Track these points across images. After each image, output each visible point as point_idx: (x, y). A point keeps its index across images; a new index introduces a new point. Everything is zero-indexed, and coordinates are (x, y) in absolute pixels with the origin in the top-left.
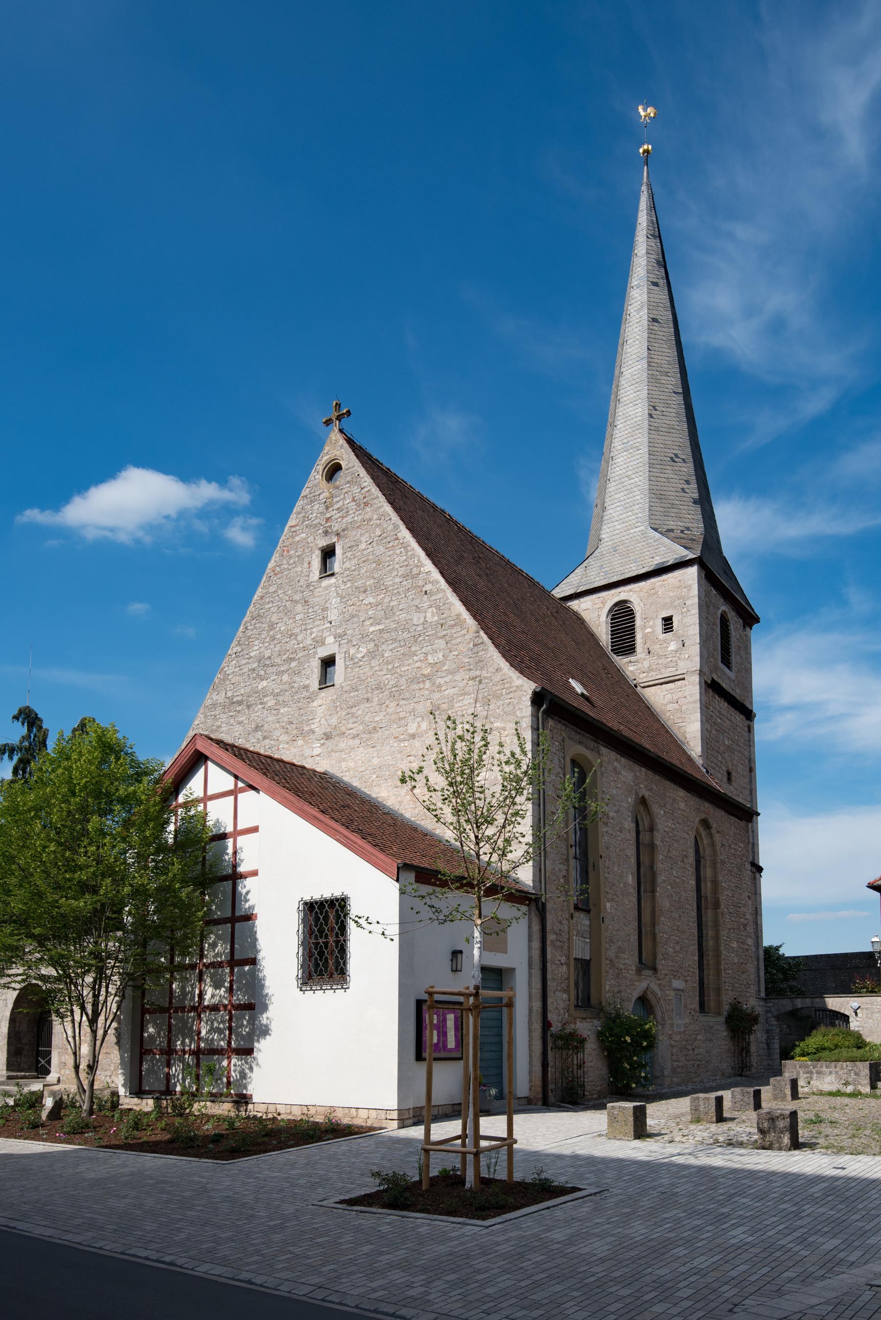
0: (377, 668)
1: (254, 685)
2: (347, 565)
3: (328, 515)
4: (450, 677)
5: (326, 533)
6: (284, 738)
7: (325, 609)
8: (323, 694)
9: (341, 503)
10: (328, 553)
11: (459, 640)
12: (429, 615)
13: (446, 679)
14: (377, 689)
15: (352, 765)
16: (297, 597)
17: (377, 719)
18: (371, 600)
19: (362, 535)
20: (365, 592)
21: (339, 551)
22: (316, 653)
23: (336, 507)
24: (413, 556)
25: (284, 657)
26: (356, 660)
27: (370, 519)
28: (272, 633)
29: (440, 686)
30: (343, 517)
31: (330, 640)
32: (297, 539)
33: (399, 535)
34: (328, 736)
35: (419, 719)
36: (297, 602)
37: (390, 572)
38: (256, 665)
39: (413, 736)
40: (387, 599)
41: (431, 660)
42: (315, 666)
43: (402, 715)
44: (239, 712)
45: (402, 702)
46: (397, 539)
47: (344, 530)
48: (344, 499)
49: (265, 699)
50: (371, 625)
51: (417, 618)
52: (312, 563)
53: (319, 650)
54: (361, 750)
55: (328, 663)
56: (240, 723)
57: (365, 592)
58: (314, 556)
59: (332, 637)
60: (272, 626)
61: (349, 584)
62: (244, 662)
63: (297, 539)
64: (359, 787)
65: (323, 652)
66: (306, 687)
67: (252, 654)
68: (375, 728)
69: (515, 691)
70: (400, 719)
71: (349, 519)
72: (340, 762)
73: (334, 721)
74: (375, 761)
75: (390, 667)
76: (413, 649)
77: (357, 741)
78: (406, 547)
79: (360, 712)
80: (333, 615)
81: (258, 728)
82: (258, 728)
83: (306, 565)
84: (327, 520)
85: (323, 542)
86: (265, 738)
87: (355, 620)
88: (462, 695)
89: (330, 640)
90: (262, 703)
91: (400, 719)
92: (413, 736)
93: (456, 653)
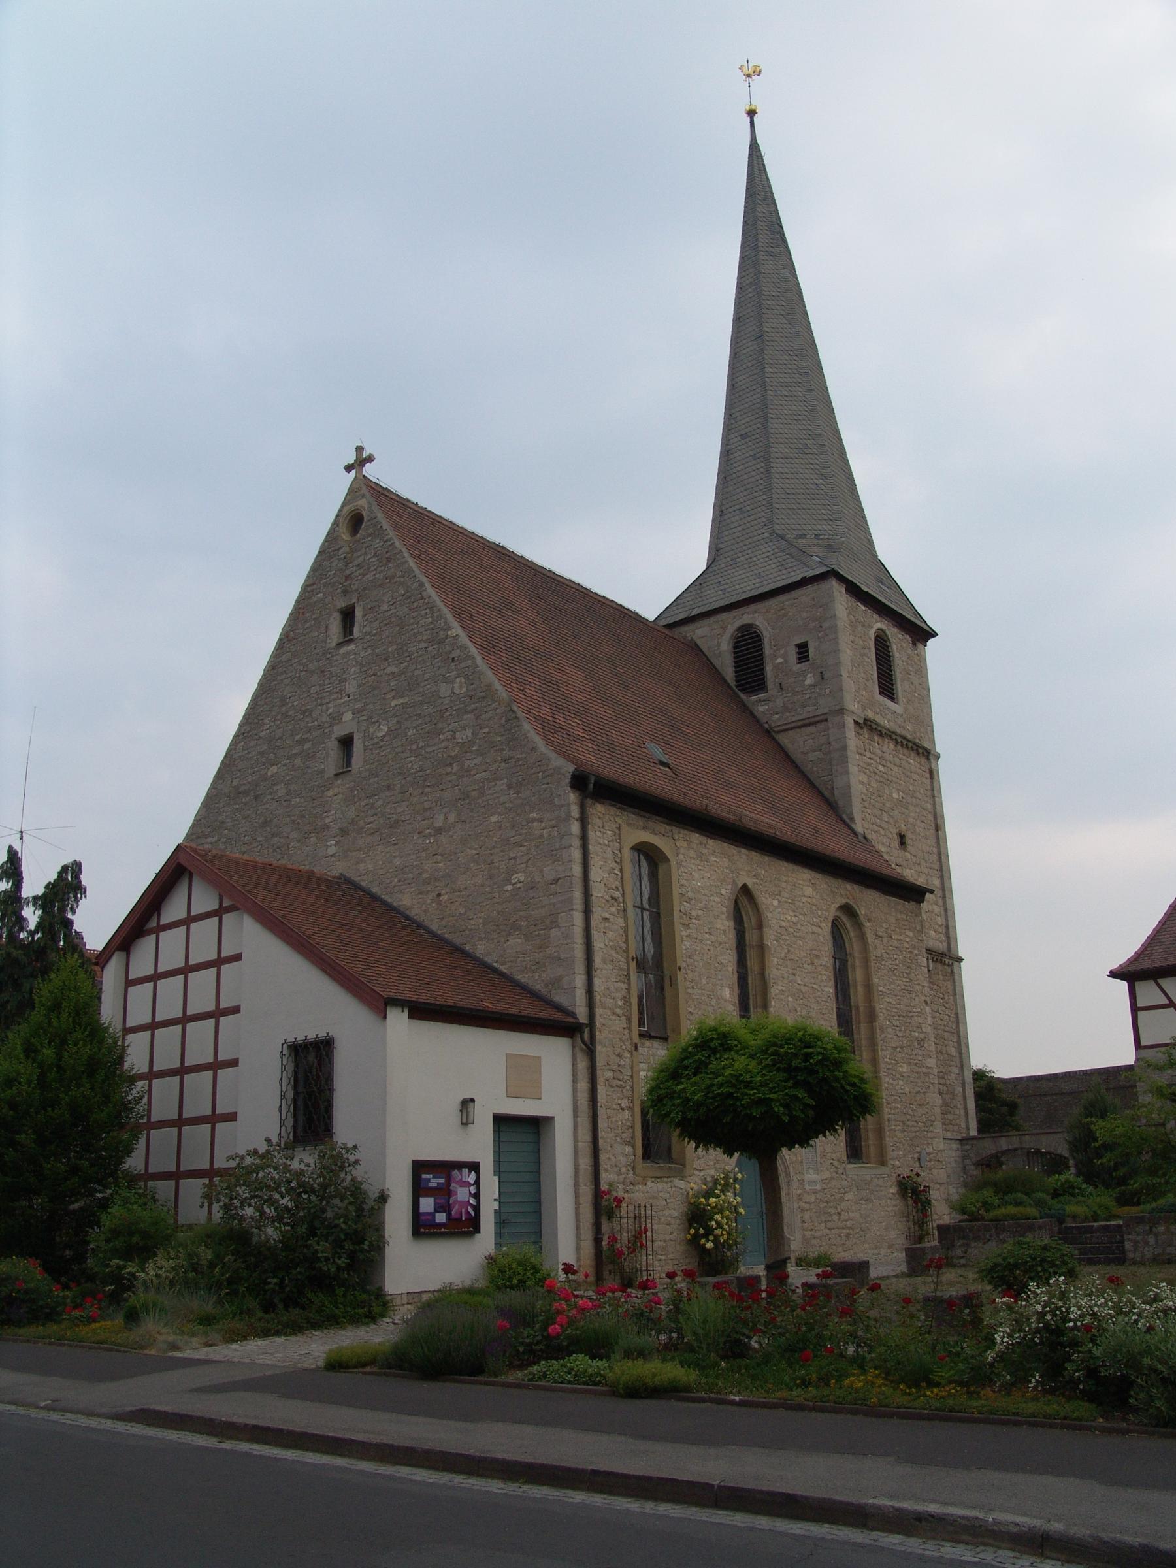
0: (400, 749)
1: (263, 772)
2: (367, 629)
3: (348, 572)
4: (480, 758)
5: (345, 592)
6: (295, 835)
7: (345, 680)
8: (339, 782)
9: (361, 558)
10: (348, 616)
11: (490, 714)
12: (456, 685)
13: (475, 761)
14: (399, 774)
15: (371, 867)
16: (311, 667)
17: (399, 810)
18: (393, 669)
19: (384, 594)
20: (386, 659)
21: (358, 613)
22: (332, 732)
23: (356, 563)
24: (441, 617)
25: (297, 737)
26: (376, 740)
27: (393, 577)
28: (284, 709)
29: (469, 770)
30: (364, 575)
31: (348, 716)
32: (314, 599)
33: (424, 594)
34: (344, 832)
35: (445, 810)
36: (312, 672)
37: (415, 635)
38: (265, 747)
39: (439, 831)
40: (412, 668)
41: (459, 737)
42: (332, 746)
43: (427, 805)
44: (245, 804)
45: (428, 789)
46: (423, 598)
47: (365, 589)
48: (365, 554)
49: (275, 788)
50: (394, 698)
51: (444, 690)
52: (330, 626)
53: (335, 728)
54: (381, 848)
55: (346, 743)
56: (246, 818)
57: (386, 659)
58: (332, 619)
59: (350, 713)
60: (284, 701)
61: (370, 651)
62: (252, 744)
63: (314, 599)
64: (379, 893)
65: (340, 731)
66: (321, 772)
67: (262, 734)
68: (396, 822)
69: (552, 775)
70: (426, 810)
71: (369, 577)
72: (357, 863)
73: (351, 813)
74: (397, 862)
75: (414, 747)
76: (440, 725)
77: (377, 837)
78: (432, 607)
79: (380, 803)
80: (351, 687)
81: (265, 824)
82: (265, 824)
83: (323, 629)
84: (347, 578)
85: (342, 603)
86: (274, 835)
87: (376, 692)
88: (494, 780)
89: (348, 716)
90: (271, 794)
91: (426, 810)
92: (439, 831)
93: (487, 730)
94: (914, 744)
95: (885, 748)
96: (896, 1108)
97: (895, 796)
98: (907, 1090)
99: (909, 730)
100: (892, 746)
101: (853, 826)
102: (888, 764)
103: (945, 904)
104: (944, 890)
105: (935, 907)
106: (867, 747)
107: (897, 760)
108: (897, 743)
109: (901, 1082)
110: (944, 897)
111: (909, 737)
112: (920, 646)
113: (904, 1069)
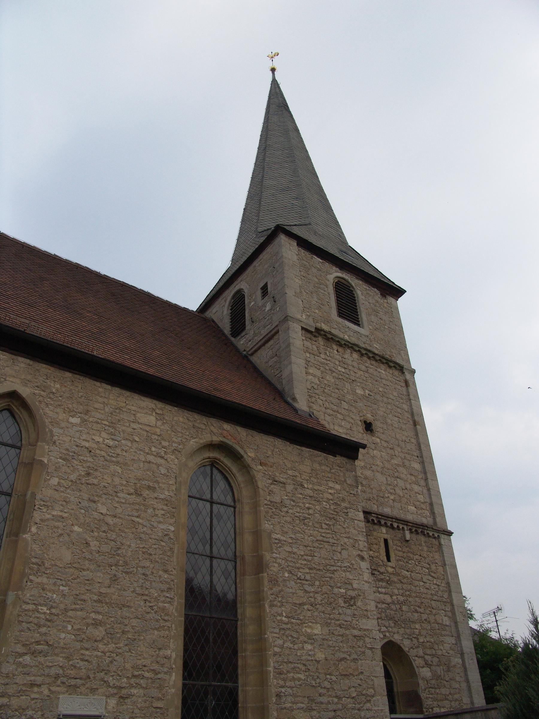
94: (383, 358)
95: (346, 356)
96: (294, 679)
97: (359, 391)
98: (320, 656)
99: (377, 348)
100: (355, 355)
101: (296, 405)
102: (351, 368)
103: (427, 485)
104: (425, 473)
105: (416, 488)
106: (322, 351)
107: (363, 368)
108: (362, 355)
109: (308, 647)
110: (426, 479)
111: (376, 352)
112: (391, 300)
113: (317, 630)
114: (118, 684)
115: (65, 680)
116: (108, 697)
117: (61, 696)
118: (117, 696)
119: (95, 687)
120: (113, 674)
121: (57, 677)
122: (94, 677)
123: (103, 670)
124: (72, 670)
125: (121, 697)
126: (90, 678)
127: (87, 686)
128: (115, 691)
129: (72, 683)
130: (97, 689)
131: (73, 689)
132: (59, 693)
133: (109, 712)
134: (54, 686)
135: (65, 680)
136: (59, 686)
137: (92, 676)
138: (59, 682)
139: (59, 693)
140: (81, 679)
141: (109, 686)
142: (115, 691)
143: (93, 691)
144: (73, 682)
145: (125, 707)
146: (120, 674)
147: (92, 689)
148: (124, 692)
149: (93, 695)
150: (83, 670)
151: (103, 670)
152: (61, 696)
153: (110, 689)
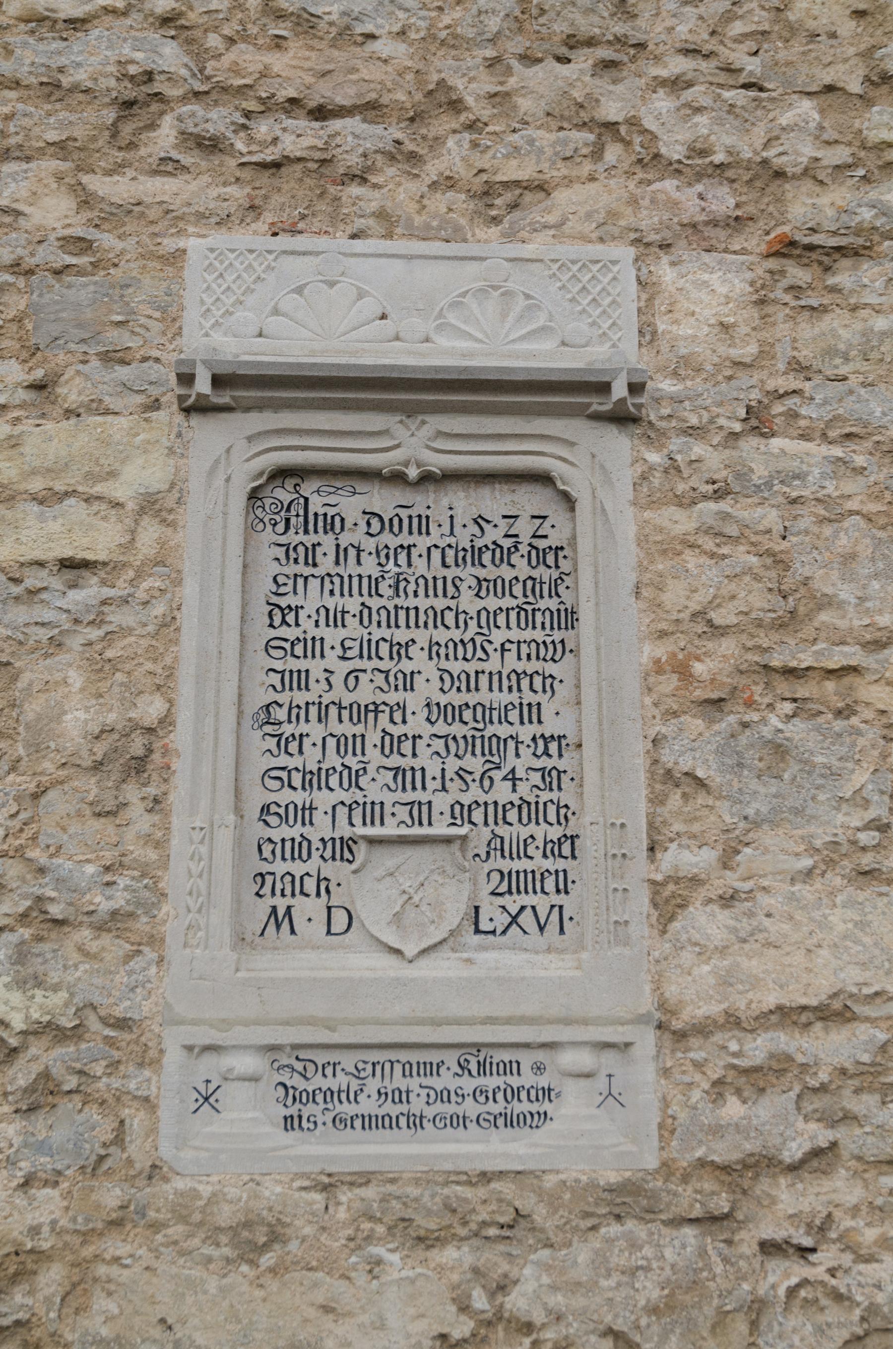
114: (726, 141)
115: (217, 119)
116: (650, 247)
117: (195, 244)
118: (754, 241)
119: (512, 171)
120: (678, 65)
121: (138, 99)
122: (499, 99)
123: (573, 42)
124: (278, 43)
125: (787, 248)
126: (456, 106)
127: (433, 169)
128: (723, 200)
129: (290, 145)
130: (542, 188)
131: (300, 188)
132: (175, 218)
133: (684, 367)
134: (117, 169)
135: (217, 119)
136: (168, 166)
137: (473, 87)
138: (165, 137)
139: (175, 218)
140: (370, 109)
141: (653, 162)
142: (723, 200)
143: (499, 200)
144: (297, 137)
145: (840, 327)
146: (753, 66)
147: (488, 192)
148: (808, 209)
149: (510, 236)
150: (381, 47)
151: (573, 42)
152: (195, 244)
153: (669, 185)
